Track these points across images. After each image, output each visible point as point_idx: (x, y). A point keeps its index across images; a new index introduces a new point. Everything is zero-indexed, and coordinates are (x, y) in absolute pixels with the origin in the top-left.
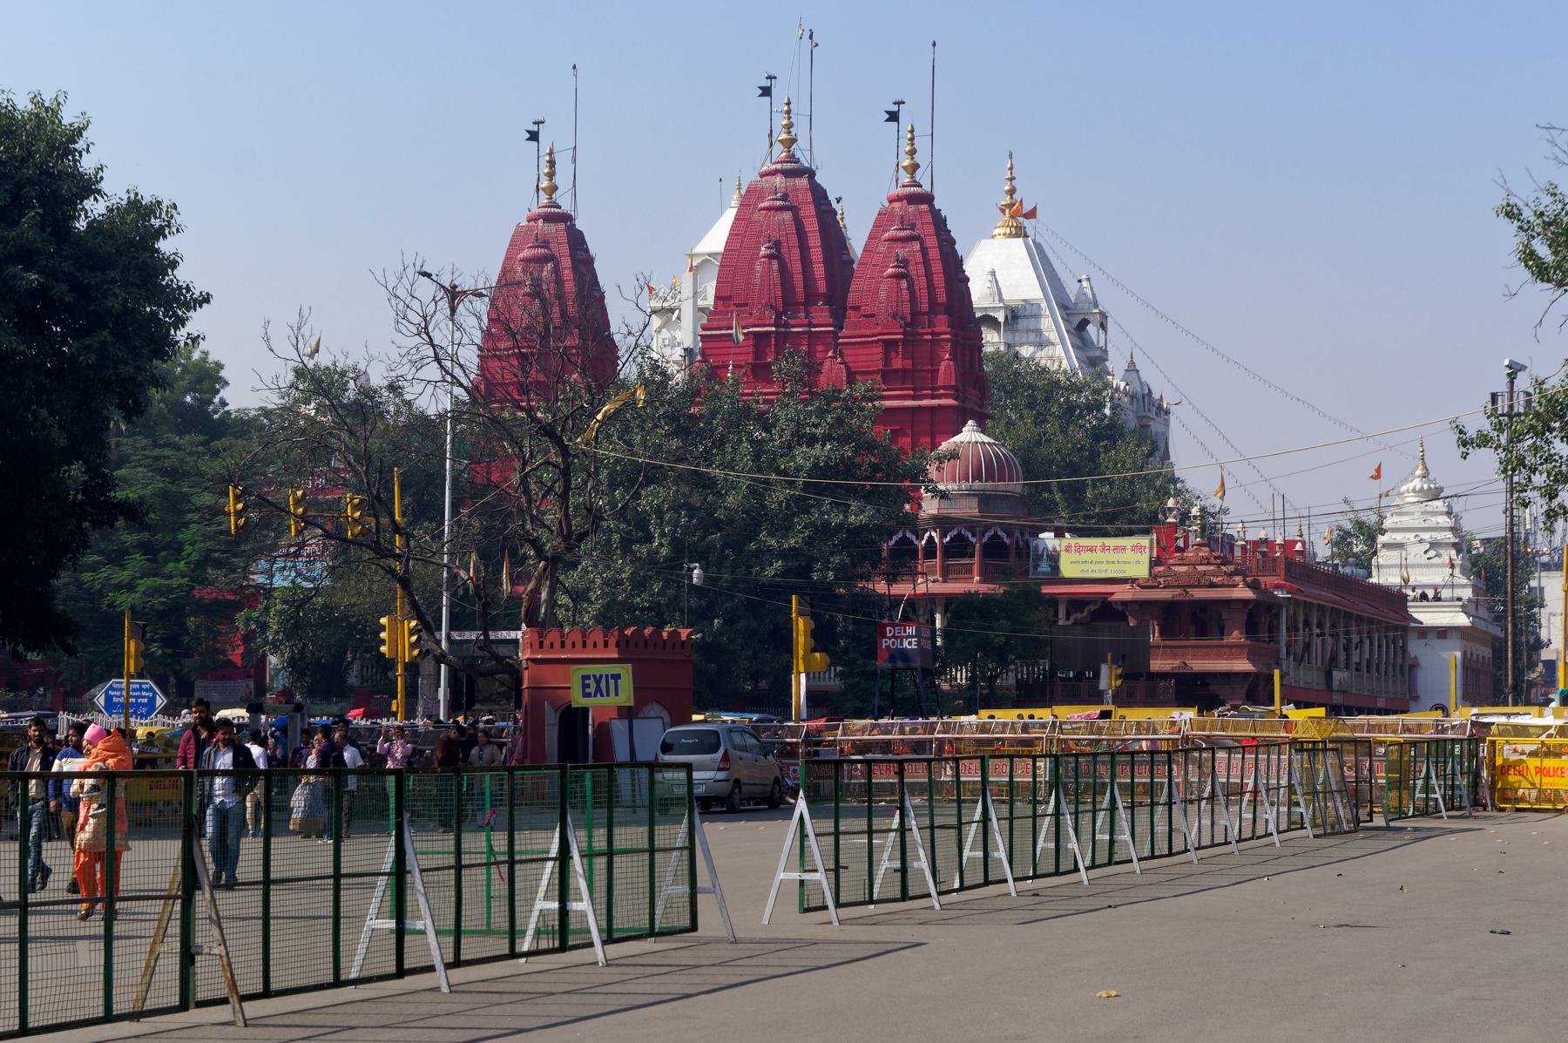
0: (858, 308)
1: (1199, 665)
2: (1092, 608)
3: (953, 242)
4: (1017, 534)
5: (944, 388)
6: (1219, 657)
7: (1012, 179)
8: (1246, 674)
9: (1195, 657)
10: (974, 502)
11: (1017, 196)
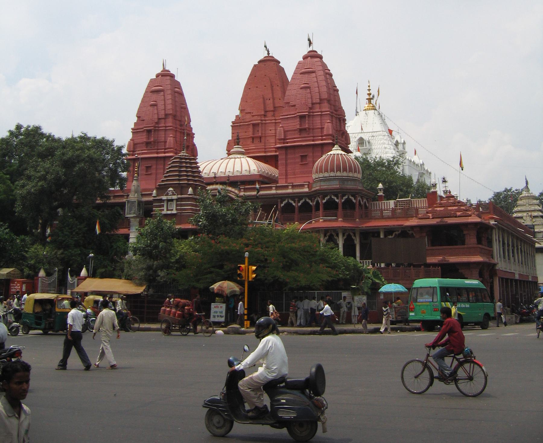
0: (289, 103)
1: (453, 259)
2: (397, 233)
3: (331, 75)
4: (359, 198)
5: (325, 136)
6: (464, 254)
7: (369, 90)
10: (337, 182)
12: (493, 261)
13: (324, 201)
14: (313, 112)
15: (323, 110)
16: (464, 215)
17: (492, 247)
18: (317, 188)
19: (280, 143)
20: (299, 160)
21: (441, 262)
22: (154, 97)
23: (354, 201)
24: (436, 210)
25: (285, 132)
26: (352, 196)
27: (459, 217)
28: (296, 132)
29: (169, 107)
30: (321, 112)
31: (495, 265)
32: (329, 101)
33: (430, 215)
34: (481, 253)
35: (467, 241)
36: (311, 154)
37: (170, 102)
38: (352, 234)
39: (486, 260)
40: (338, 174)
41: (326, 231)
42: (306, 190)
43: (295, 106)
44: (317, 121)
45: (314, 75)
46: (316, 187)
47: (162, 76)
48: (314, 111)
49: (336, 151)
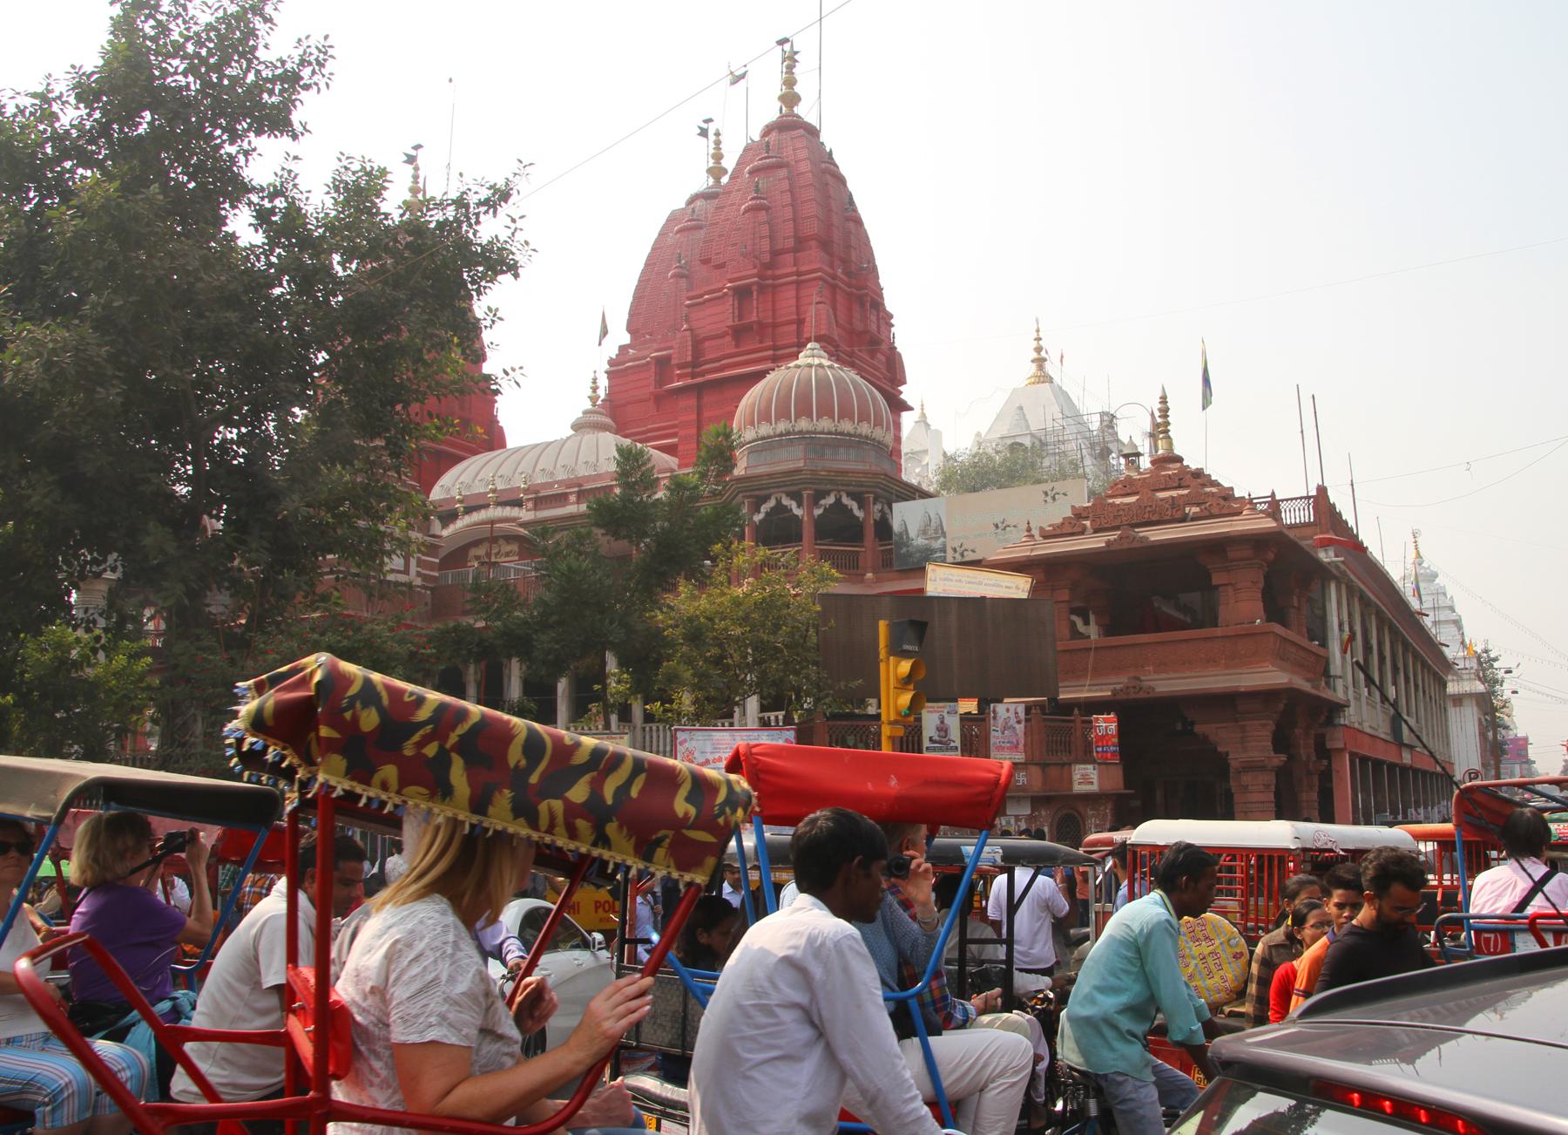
1: (1166, 684)
7: (1038, 339)
8: (1268, 696)
11: (1043, 354)
12: (1327, 694)
13: (758, 518)
14: (775, 277)
15: (803, 269)
17: (1324, 644)
19: (680, 377)
23: (859, 514)
24: (1113, 505)
26: (850, 495)
27: (1195, 518)
28: (728, 338)
30: (799, 274)
32: (825, 244)
33: (1088, 523)
34: (1282, 656)
35: (1224, 613)
39: (1306, 687)
40: (804, 424)
44: (787, 298)
45: (783, 173)
48: (778, 272)
49: (812, 358)
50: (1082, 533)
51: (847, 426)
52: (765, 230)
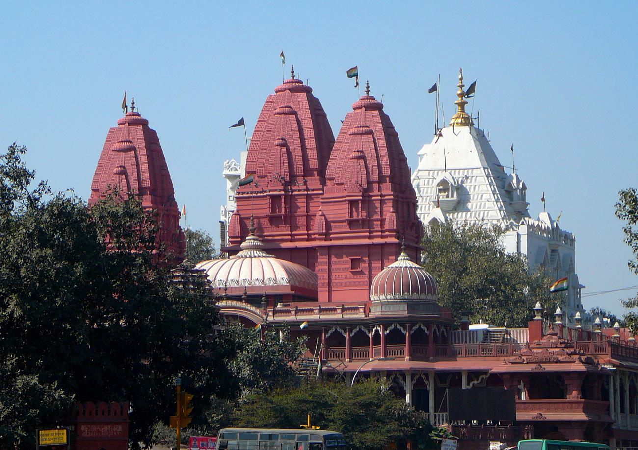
0: (333, 179)
4: (435, 328)
9: (548, 410)
12: (605, 418)
16: (567, 360)
18: (377, 314)
20: (349, 266)
21: (536, 420)
22: (120, 159)
25: (328, 224)
26: (425, 325)
29: (146, 176)
31: (610, 424)
33: (524, 358)
36: (366, 259)
37: (145, 168)
38: (423, 377)
41: (389, 373)
42: (362, 316)
43: (342, 184)
46: (375, 313)
47: (129, 124)
50: (522, 363)
51: (423, 296)
52: (364, 170)
